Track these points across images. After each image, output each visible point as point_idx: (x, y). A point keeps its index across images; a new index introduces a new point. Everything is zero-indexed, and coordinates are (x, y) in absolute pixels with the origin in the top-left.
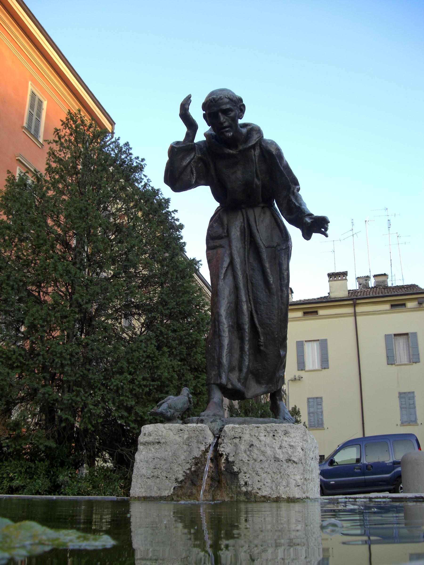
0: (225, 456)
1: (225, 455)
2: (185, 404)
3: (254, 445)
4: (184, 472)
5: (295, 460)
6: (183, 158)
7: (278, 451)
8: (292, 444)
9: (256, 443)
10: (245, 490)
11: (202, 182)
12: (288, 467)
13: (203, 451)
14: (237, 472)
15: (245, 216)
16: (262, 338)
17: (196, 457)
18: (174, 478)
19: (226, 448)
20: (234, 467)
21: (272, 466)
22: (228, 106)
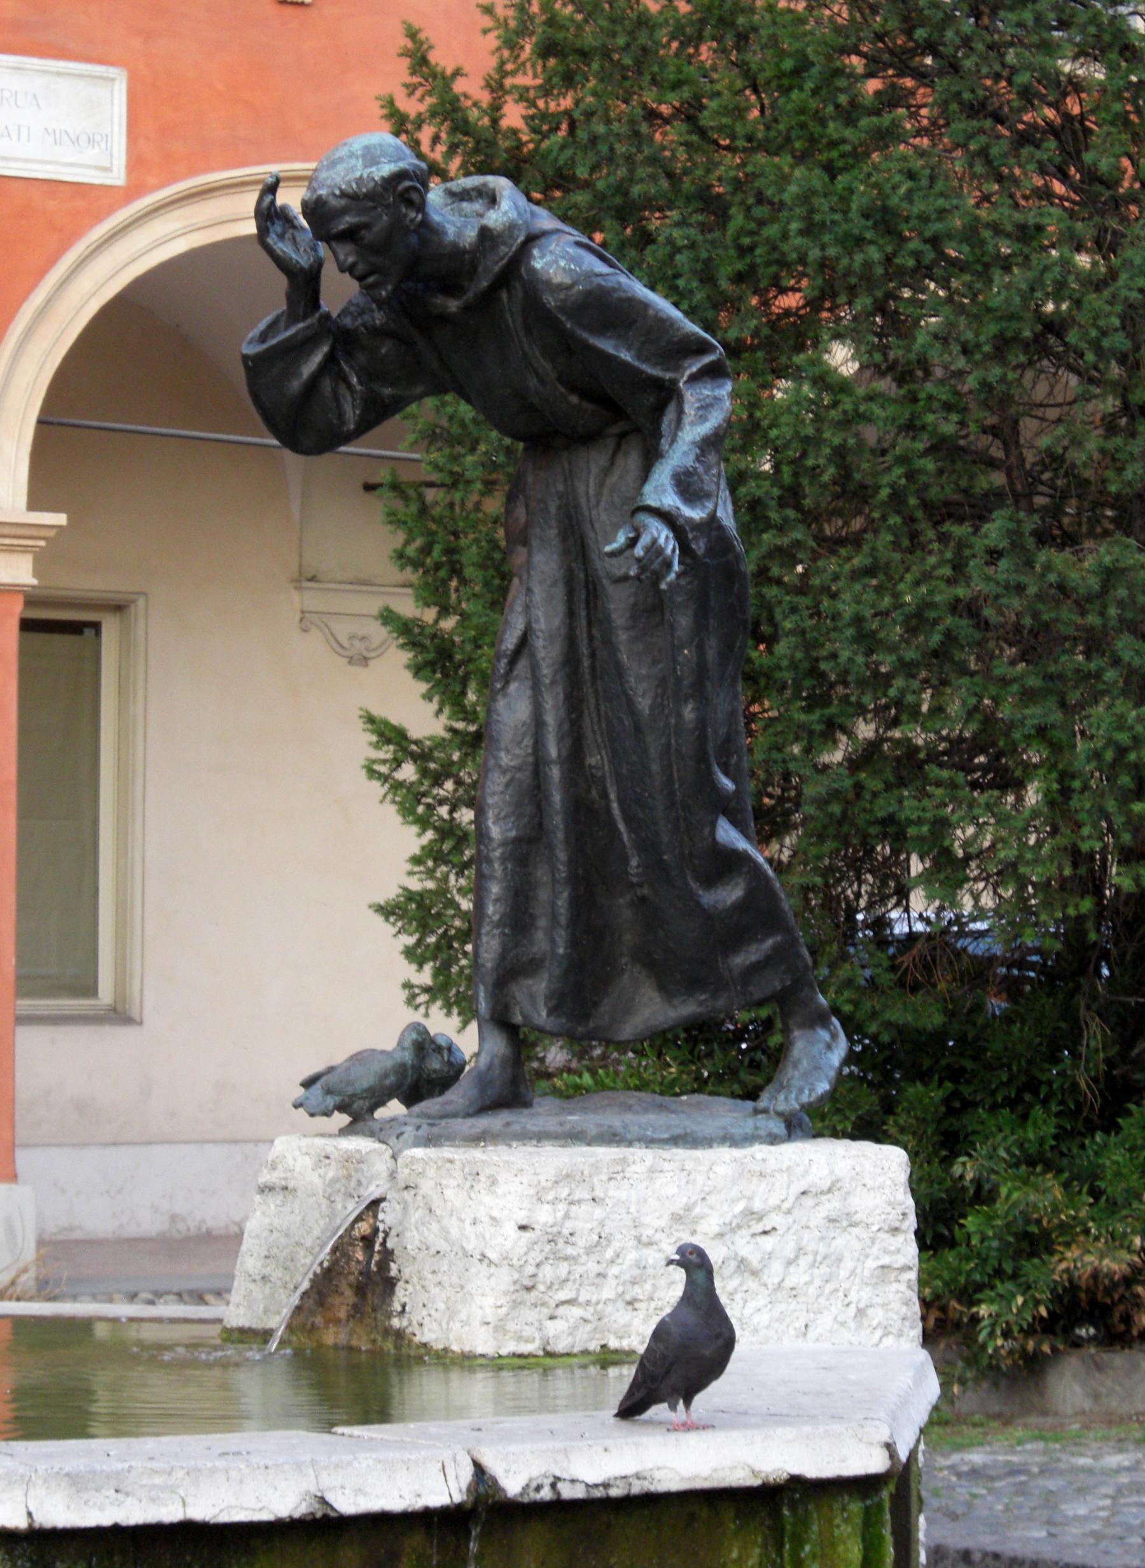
2: (386, 1075)
5: (493, 1255)
6: (291, 371)
8: (495, 1214)
11: (419, 390)
16: (634, 862)
20: (392, 1265)
22: (349, 220)
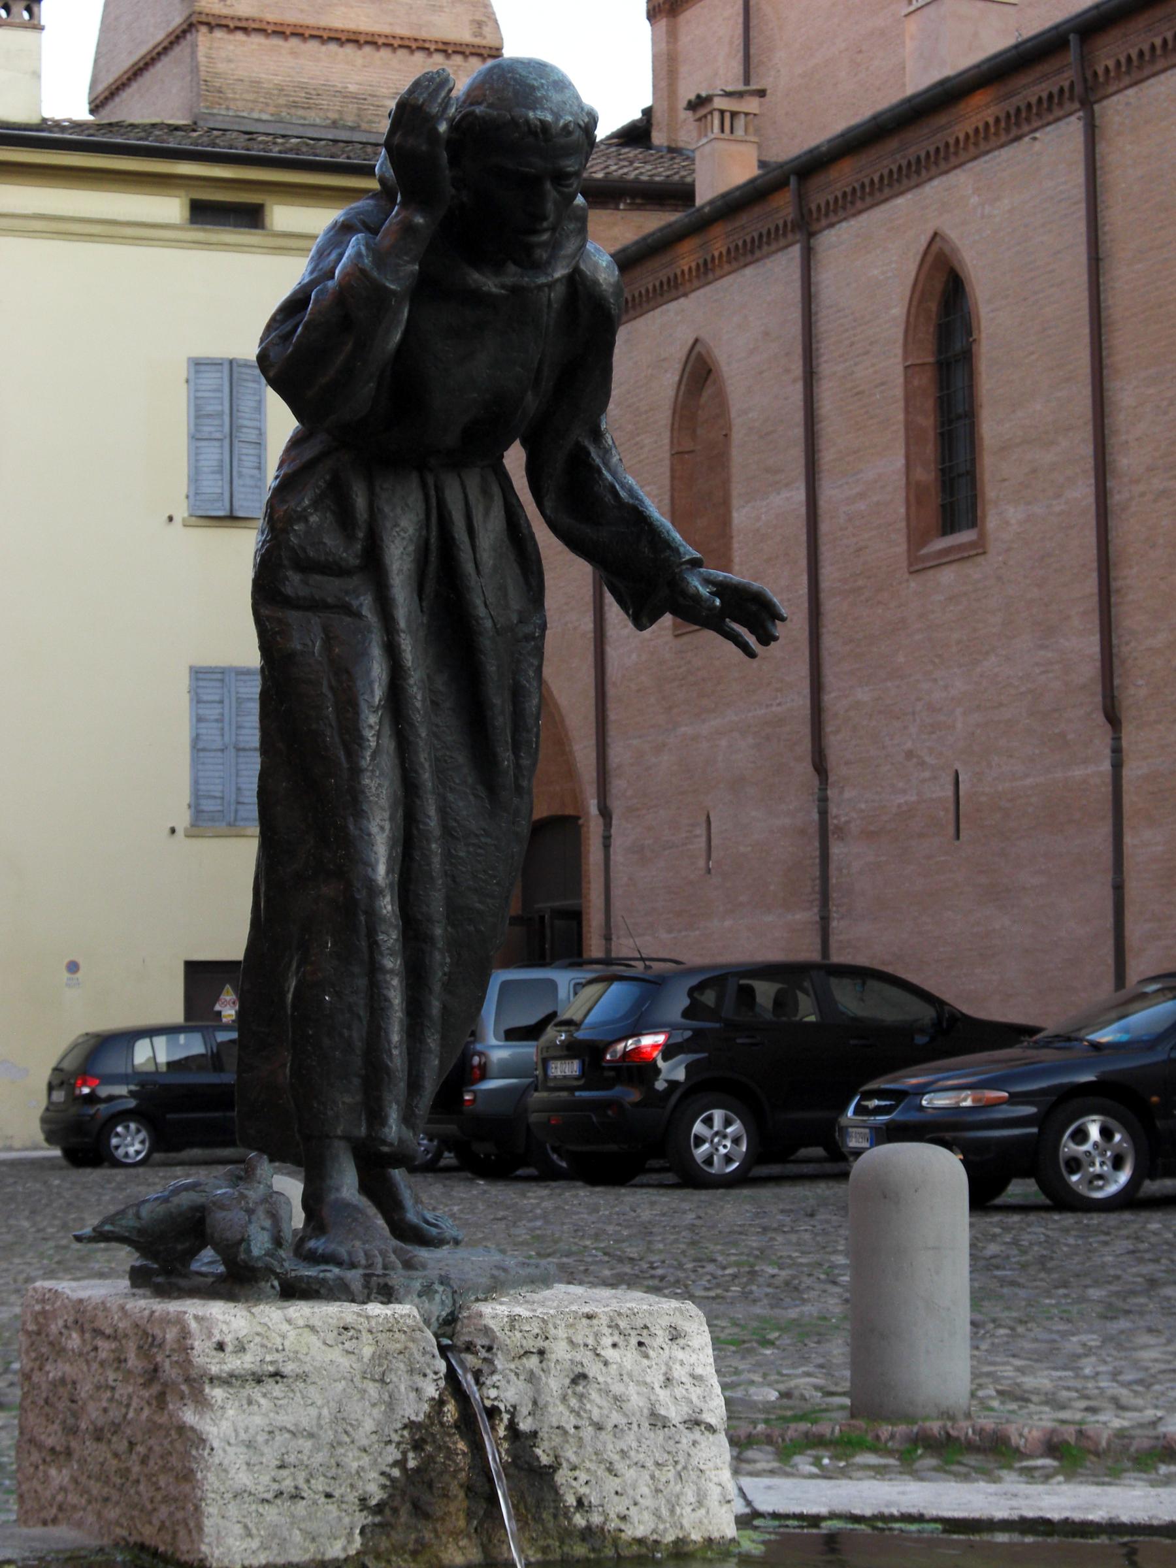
0: (506, 1417)
1: (507, 1411)
3: (591, 1375)
4: (383, 1474)
7: (663, 1395)
9: (593, 1369)
10: (583, 1523)
12: (695, 1443)
13: (433, 1399)
14: (550, 1467)
15: (434, 501)
17: (412, 1422)
18: (352, 1497)
19: (505, 1390)
20: (539, 1451)
21: (648, 1442)
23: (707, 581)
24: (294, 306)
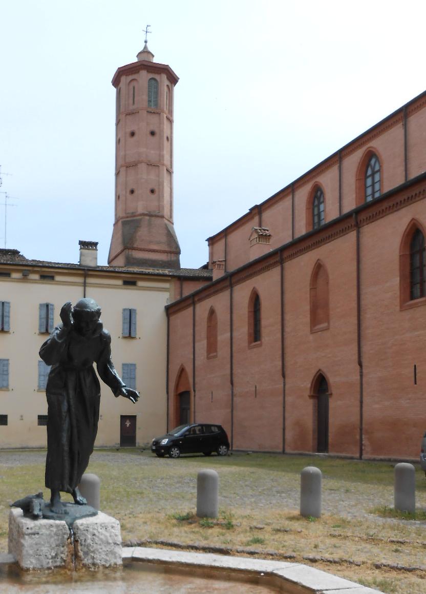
5: (119, 543)
9: (97, 534)
23: (125, 390)
24: (45, 343)
